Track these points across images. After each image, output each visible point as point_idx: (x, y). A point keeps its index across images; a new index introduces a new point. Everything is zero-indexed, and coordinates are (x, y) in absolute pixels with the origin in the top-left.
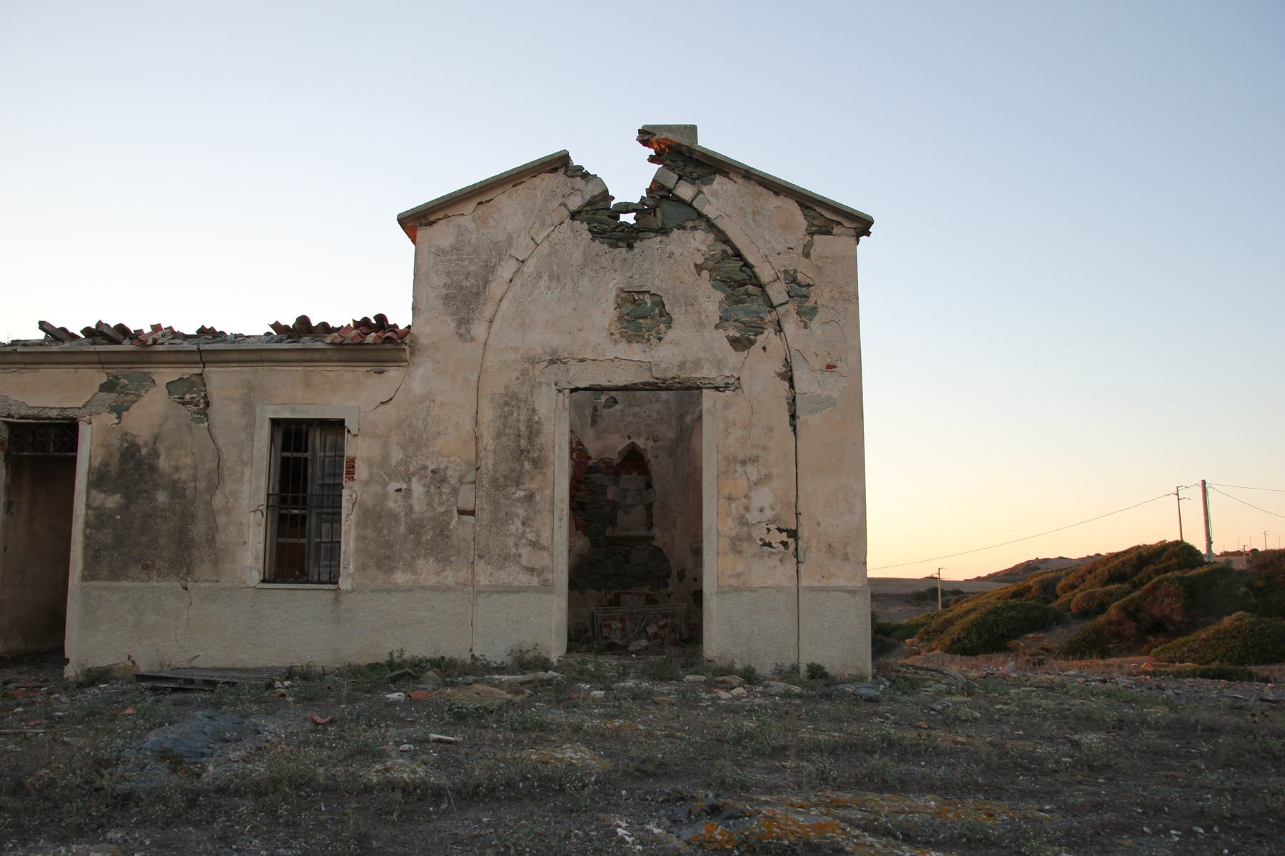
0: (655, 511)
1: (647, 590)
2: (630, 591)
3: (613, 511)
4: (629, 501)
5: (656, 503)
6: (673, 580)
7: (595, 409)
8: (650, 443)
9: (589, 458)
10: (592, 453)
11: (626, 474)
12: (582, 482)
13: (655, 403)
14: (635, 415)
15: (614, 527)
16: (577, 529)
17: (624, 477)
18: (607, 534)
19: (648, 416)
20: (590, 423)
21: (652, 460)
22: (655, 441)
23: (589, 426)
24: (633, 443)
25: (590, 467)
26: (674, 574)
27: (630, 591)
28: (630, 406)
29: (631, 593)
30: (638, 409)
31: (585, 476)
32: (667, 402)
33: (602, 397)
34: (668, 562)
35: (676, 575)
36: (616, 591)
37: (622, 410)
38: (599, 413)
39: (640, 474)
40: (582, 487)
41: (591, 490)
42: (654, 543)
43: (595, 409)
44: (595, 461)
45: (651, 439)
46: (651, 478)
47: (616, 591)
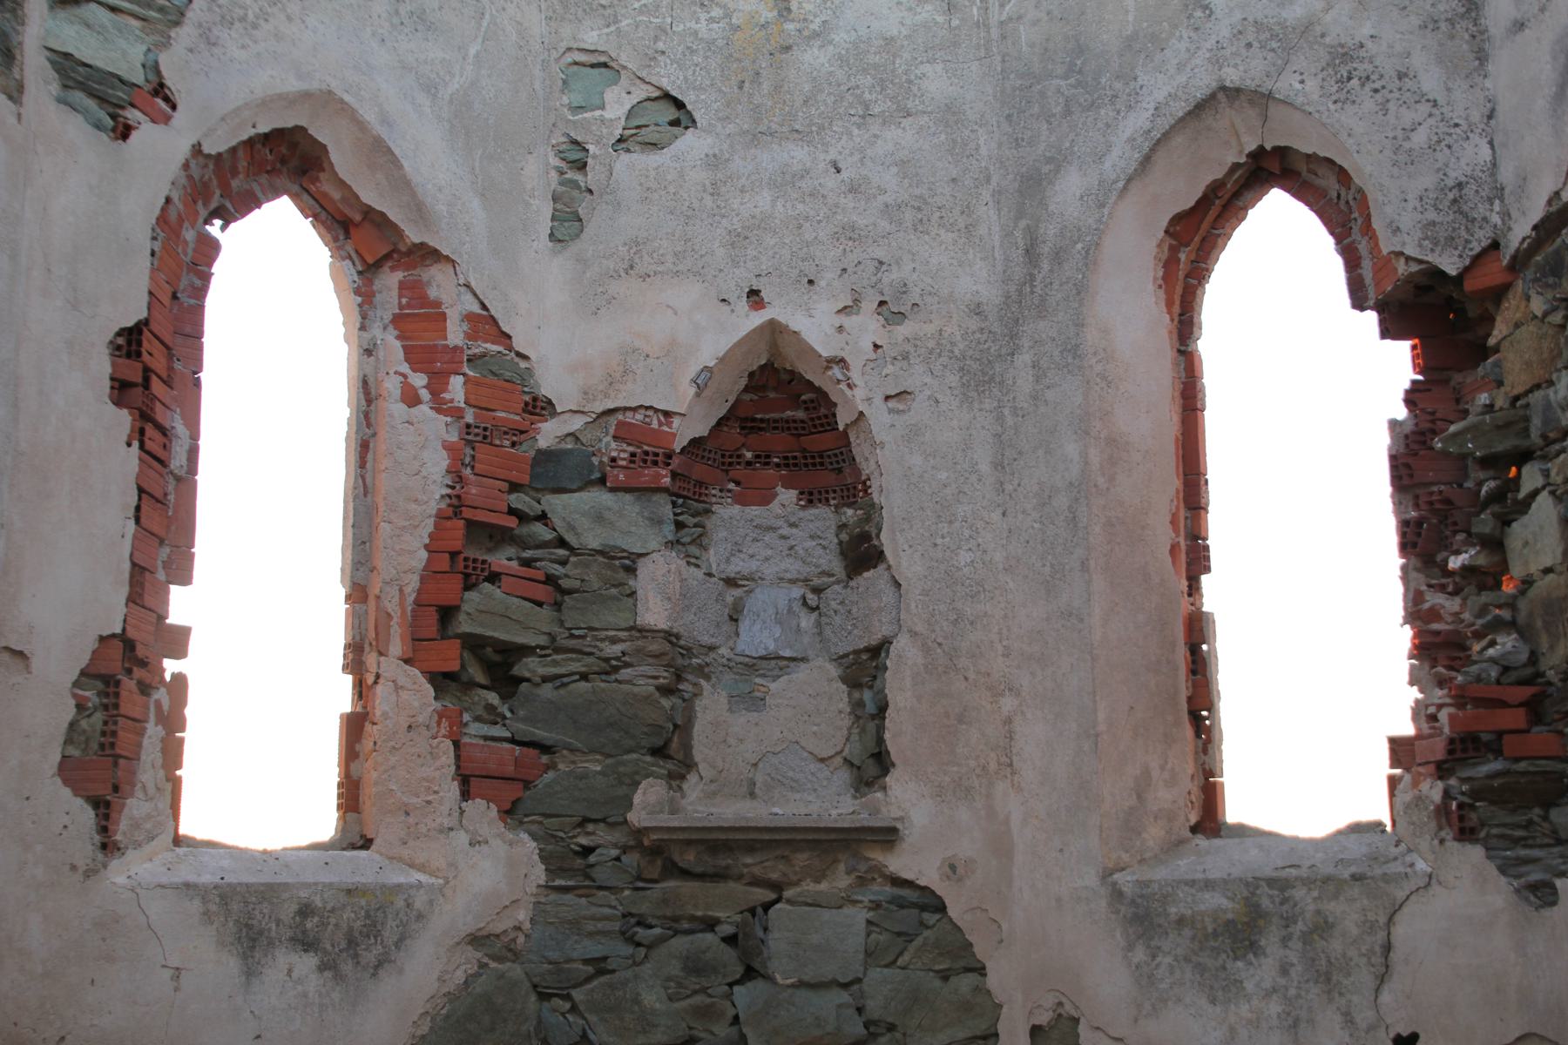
0: (900, 686)
3: (667, 691)
4: (757, 637)
5: (901, 644)
7: (576, 158)
8: (867, 327)
9: (540, 407)
10: (553, 382)
11: (742, 500)
12: (497, 536)
14: (785, 181)
15: (676, 778)
16: (466, 795)
17: (729, 518)
18: (637, 817)
19: (853, 189)
20: (545, 225)
21: (879, 418)
22: (889, 312)
23: (543, 241)
24: (774, 329)
25: (545, 456)
28: (756, 138)
30: (798, 154)
31: (519, 501)
32: (950, 114)
33: (611, 95)
34: (981, 970)
37: (714, 162)
38: (593, 177)
39: (810, 498)
40: (502, 560)
41: (550, 580)
42: (899, 863)
43: (576, 158)
44: (577, 423)
45: (869, 305)
46: (872, 512)
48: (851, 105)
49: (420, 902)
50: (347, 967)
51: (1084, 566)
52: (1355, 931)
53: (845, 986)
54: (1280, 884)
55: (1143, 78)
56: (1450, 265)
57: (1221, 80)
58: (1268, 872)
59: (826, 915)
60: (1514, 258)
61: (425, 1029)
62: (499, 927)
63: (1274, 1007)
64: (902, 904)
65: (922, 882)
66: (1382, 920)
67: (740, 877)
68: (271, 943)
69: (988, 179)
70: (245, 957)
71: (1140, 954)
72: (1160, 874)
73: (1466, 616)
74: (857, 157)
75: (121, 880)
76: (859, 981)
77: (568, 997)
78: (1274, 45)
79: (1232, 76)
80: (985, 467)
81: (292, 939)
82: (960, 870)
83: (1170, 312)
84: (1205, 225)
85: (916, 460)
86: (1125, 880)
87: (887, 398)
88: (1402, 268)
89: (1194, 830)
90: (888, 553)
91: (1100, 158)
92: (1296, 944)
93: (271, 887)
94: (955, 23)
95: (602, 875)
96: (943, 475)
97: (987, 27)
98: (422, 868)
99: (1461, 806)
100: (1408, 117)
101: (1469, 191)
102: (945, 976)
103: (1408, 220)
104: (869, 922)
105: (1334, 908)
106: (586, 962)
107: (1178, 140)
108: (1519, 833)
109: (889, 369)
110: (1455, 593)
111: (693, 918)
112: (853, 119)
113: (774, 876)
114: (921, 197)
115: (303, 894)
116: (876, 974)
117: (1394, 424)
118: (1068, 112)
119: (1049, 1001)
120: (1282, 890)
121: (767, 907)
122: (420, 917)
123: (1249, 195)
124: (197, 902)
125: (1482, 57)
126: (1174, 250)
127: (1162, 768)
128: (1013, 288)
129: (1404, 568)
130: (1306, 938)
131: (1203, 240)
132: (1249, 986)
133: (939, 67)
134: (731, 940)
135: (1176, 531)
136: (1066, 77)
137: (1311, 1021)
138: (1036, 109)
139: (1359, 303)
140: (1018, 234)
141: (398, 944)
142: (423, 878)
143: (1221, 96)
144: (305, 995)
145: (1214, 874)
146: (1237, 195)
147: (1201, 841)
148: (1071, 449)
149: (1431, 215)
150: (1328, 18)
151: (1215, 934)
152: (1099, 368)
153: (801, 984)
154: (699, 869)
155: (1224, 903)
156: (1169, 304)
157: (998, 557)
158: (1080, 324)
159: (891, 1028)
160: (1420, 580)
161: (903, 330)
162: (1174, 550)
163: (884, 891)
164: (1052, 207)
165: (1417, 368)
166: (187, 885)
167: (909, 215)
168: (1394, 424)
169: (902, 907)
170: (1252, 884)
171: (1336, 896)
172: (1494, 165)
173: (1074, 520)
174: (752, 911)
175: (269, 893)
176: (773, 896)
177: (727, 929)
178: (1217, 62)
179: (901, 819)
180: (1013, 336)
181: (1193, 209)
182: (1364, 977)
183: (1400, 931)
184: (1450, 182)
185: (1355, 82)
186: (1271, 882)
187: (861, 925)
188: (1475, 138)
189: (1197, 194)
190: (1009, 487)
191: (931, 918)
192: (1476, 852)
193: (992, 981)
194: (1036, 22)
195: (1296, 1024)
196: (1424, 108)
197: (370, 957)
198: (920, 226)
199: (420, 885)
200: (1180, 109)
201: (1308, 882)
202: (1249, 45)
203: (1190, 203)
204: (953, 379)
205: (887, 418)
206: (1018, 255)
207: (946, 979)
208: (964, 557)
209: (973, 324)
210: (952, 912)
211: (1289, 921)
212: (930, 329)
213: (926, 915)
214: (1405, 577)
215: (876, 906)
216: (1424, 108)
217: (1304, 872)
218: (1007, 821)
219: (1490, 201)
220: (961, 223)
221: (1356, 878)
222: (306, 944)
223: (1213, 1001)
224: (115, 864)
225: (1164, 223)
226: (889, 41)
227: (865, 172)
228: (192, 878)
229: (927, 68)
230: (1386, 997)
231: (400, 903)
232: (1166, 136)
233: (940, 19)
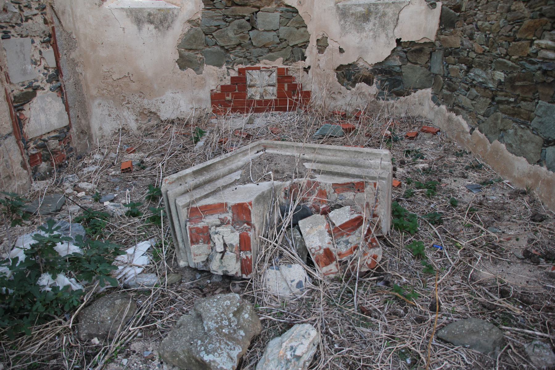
1: (279, 63)
2: (257, 65)
6: (311, 51)
26: (313, 43)
27: (257, 65)
29: (259, 69)
34: (306, 27)
35: (315, 43)
36: (241, 66)
47: (241, 66)
49: (176, 12)
50: (161, 28)
52: (391, 15)
53: (275, 31)
59: (270, 14)
61: (180, 42)
62: (194, 18)
63: (371, 33)
64: (288, 11)
66: (398, 13)
67: (250, 5)
68: (143, 22)
70: (138, 25)
71: (342, 22)
75: (107, 7)
76: (278, 29)
77: (211, 35)
81: (148, 21)
82: (302, 3)
86: (340, 5)
92: (378, 19)
93: (141, 9)
95: (217, 5)
98: (175, 4)
102: (298, 28)
104: (280, 16)
105: (387, 10)
106: (215, 26)
111: (239, 15)
113: (258, 5)
115: (149, 10)
116: (282, 28)
119: (321, 33)
120: (376, 6)
121: (256, 12)
122: (176, 16)
124: (125, 12)
130: (380, 17)
132: (366, 29)
134: (248, 21)
137: (379, 36)
141: (172, 22)
142: (176, 7)
144: (153, 34)
145: (361, 3)
151: (360, 17)
153: (265, 31)
154: (240, 4)
155: (363, 10)
159: (285, 40)
163: (283, 8)
166: (122, 8)
169: (288, 12)
170: (370, 5)
171: (388, 8)
174: (253, 13)
175: (141, 10)
176: (258, 10)
177: (247, 18)
182: (392, 26)
183: (401, 15)
186: (374, 4)
187: (279, 16)
191: (295, 15)
193: (308, 29)
195: (375, 37)
197: (166, 25)
199: (175, 8)
207: (298, 29)
210: (300, 13)
211: (377, 13)
215: (282, 12)
222: (151, 22)
223: (358, 33)
224: (105, 3)
228: (123, 7)
230: (396, 30)
231: (171, 13)
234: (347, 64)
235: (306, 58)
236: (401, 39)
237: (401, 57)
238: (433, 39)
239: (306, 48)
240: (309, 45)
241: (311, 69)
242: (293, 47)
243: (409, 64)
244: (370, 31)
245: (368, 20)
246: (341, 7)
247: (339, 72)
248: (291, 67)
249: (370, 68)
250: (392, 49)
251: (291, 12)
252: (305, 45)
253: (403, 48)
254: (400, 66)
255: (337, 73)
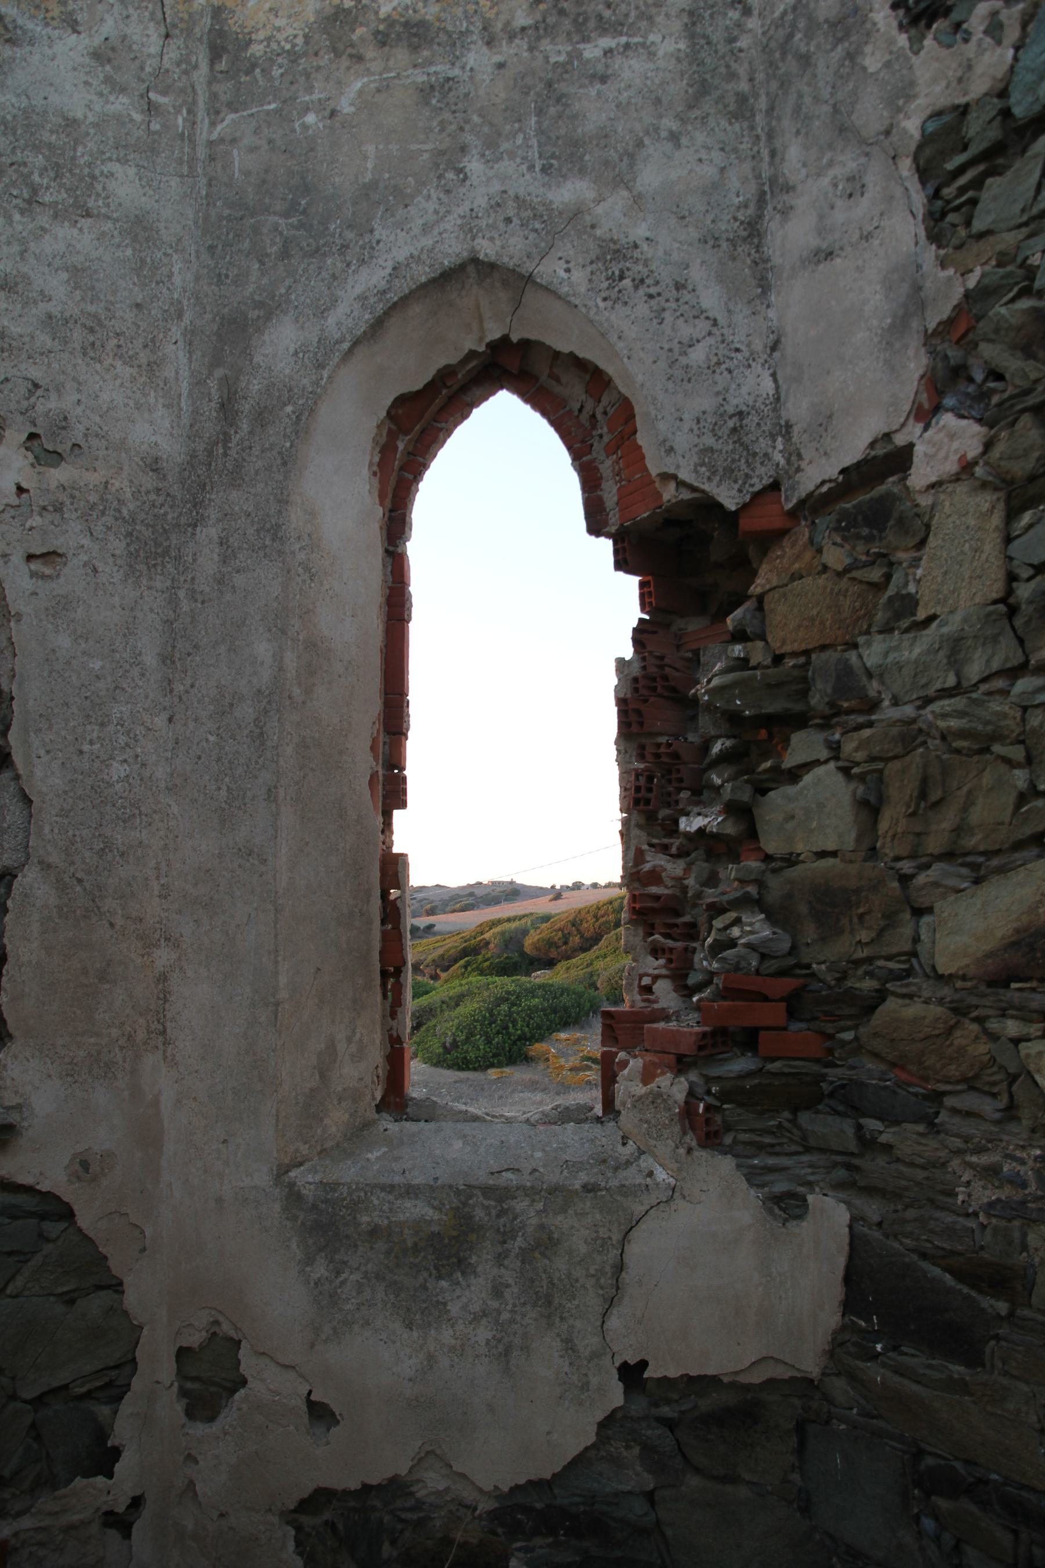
13: (58, 215)
34: (117, 1286)
35: (167, 1370)
48: (14, 184)
51: (271, 794)
52: (583, 1249)
54: (500, 1195)
55: (380, 233)
56: (729, 498)
57: (473, 250)
58: (482, 1177)
60: (802, 503)
63: (483, 1333)
65: (43, 1187)
66: (616, 1237)
69: (180, 316)
71: (320, 1270)
72: (347, 1172)
73: (691, 882)
74: (16, 248)
78: (538, 225)
79: (487, 249)
80: (150, 660)
82: (94, 1168)
83: (382, 504)
84: (428, 415)
85: (64, 641)
86: (304, 1178)
87: (30, 557)
88: (669, 493)
89: (379, 1108)
90: (17, 758)
91: (322, 313)
94: (155, 126)
96: (96, 664)
97: (192, 142)
99: (708, 1108)
100: (686, 331)
101: (751, 421)
102: (70, 1301)
103: (682, 441)
105: (560, 1222)
107: (417, 309)
108: (768, 1140)
109: (36, 521)
110: (678, 856)
112: (15, 201)
114: (95, 316)
117: (621, 663)
118: (285, 254)
120: (500, 1200)
123: (478, 392)
125: (765, 287)
126: (392, 436)
127: (349, 1040)
128: (201, 447)
129: (625, 823)
130: (525, 1256)
131: (423, 431)
132: (454, 1309)
133: (132, 171)
135: (376, 758)
136: (286, 215)
138: (246, 245)
139: (595, 527)
140: (213, 384)
143: (471, 269)
145: (418, 1179)
146: (464, 388)
147: (388, 1124)
148: (263, 649)
149: (709, 441)
150: (600, 210)
151: (416, 1249)
152: (301, 556)
155: (430, 1213)
156: (382, 496)
157: (161, 772)
158: (284, 502)
160: (640, 837)
161: (58, 475)
162: (374, 776)
164: (258, 359)
165: (643, 608)
167: (78, 336)
168: (621, 663)
169: (15, 1218)
171: (563, 1210)
172: (778, 399)
173: (260, 737)
178: (469, 228)
179: (18, 1107)
180: (197, 504)
181: (418, 393)
183: (635, 1249)
184: (731, 410)
185: (627, 282)
186: (487, 1191)
188: (756, 367)
189: (428, 377)
190: (179, 688)
191: (53, 1228)
192: (726, 1164)
193: (131, 1299)
194: (253, 149)
196: (703, 326)
198: (91, 350)
200: (423, 274)
201: (531, 1193)
202: (508, 220)
203: (418, 386)
204: (118, 546)
205: (27, 584)
206: (210, 409)
207: (72, 1302)
208: (118, 770)
209: (149, 481)
210: (84, 1220)
211: (506, 1236)
212: (94, 478)
213: (47, 1226)
214: (625, 835)
216: (703, 326)
217: (527, 1181)
218: (156, 1102)
219: (773, 437)
220: (143, 358)
221: (589, 1189)
223: (409, 1326)
225: (389, 402)
226: (71, 123)
227: (25, 270)
229: (116, 167)
230: (614, 1322)
232: (404, 301)
233: (138, 117)
234: (354, 1485)
235: (116, 1453)
236: (643, 1364)
237: (648, 1449)
238: (811, 1365)
239: (120, 1398)
240: (136, 1383)
241: (147, 1512)
242: (39, 1401)
243: (694, 1481)
244: (476, 1319)
245: (462, 1265)
246: (308, 1192)
247: (305, 1520)
248: (26, 1523)
249: (485, 1506)
250: (600, 1416)
251: (32, 1214)
252: (110, 1384)
253: (656, 1405)
254: (650, 1497)
255: (299, 1529)
